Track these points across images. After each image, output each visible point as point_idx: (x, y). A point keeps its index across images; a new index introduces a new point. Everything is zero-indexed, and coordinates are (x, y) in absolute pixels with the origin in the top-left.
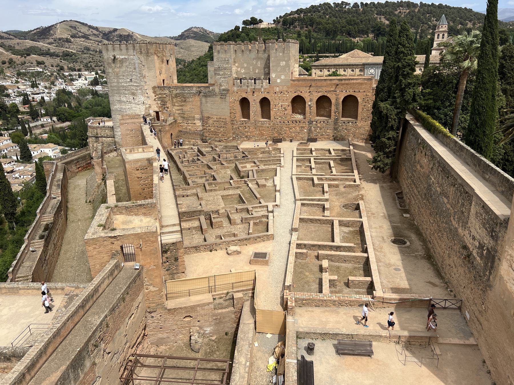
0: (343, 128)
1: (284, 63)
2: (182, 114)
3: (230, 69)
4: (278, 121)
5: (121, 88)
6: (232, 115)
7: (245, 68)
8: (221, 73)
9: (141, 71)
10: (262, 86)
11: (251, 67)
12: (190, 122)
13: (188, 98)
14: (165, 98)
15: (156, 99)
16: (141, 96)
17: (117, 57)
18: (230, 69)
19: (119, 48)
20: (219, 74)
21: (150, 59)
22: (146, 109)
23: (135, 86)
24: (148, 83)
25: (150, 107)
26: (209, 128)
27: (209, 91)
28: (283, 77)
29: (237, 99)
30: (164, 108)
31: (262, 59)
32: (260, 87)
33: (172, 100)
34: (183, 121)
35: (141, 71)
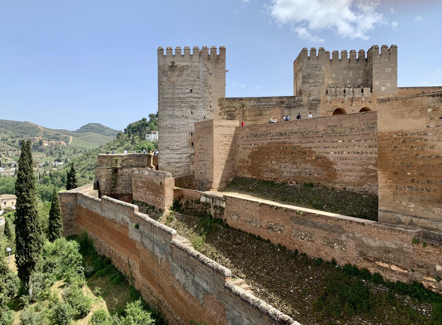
1: (390, 69)
5: (177, 100)
8: (311, 81)
9: (206, 80)
11: (341, 78)
15: (222, 113)
16: (202, 110)
17: (177, 63)
20: (308, 83)
21: (219, 66)
23: (196, 97)
24: (213, 95)
27: (294, 102)
28: (388, 85)
32: (360, 96)
33: (243, 114)
35: (206, 80)
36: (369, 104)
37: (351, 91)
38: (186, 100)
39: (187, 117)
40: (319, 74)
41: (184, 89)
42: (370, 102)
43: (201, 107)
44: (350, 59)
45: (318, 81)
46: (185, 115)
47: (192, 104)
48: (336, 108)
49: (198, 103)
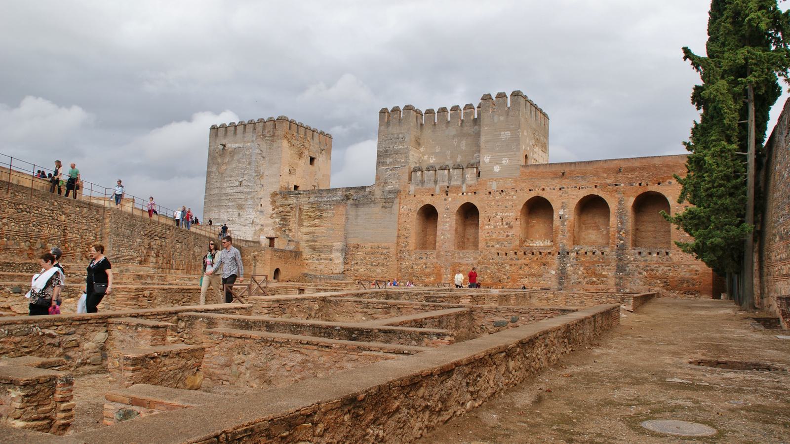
0: (637, 266)
1: (508, 133)
2: (313, 240)
3: (406, 153)
4: (493, 251)
5: (224, 198)
6: (402, 240)
7: (436, 154)
8: (388, 161)
9: (257, 167)
11: (449, 152)
12: (323, 256)
13: (326, 210)
14: (288, 212)
15: (274, 215)
17: (228, 146)
18: (406, 153)
19: (233, 132)
20: (384, 164)
21: (275, 145)
22: (255, 234)
24: (264, 188)
25: (262, 230)
26: (356, 267)
27: (363, 196)
28: (505, 161)
30: (285, 231)
32: (459, 183)
34: (313, 254)
35: (257, 167)
38: (234, 197)
39: (233, 222)
41: (232, 181)
42: (475, 193)
43: (250, 206)
44: (462, 121)
45: (399, 160)
46: (230, 219)
47: (240, 202)
49: (246, 200)
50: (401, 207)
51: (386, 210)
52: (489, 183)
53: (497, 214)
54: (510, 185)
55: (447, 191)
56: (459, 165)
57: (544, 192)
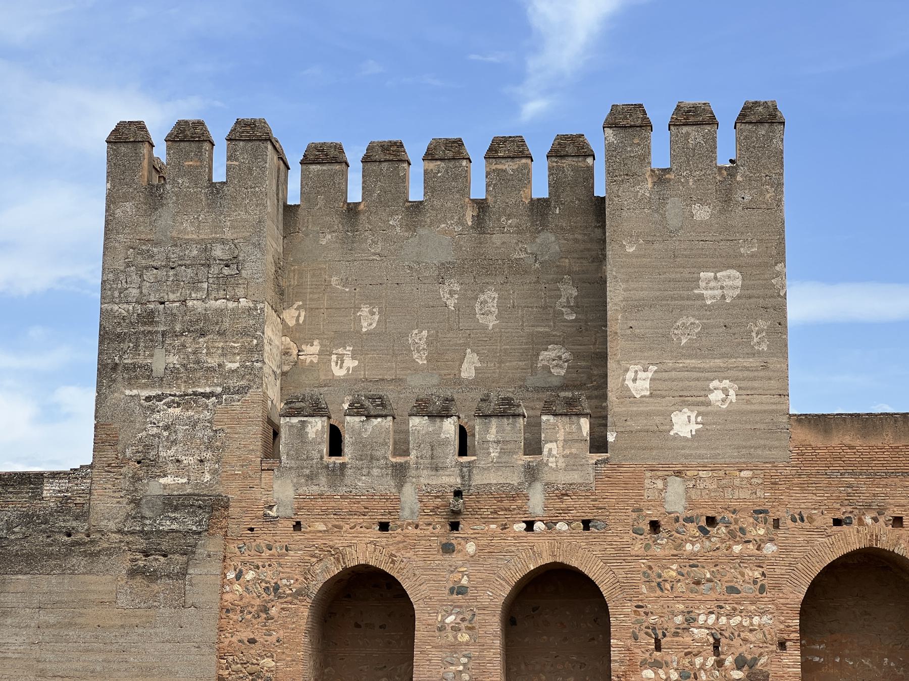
3: (245, 333)
10: (532, 473)
11: (419, 337)
18: (245, 333)
27: (28, 519)
29: (290, 583)
31: (517, 269)
32: (515, 479)
36: (582, 539)
37: (446, 442)
40: (220, 312)
42: (586, 524)
44: (481, 206)
45: (213, 362)
48: (336, 570)
50: (231, 575)
51: (155, 587)
52: (652, 485)
53: (690, 620)
54: (745, 494)
55: (457, 513)
56: (508, 402)
57: (898, 531)
